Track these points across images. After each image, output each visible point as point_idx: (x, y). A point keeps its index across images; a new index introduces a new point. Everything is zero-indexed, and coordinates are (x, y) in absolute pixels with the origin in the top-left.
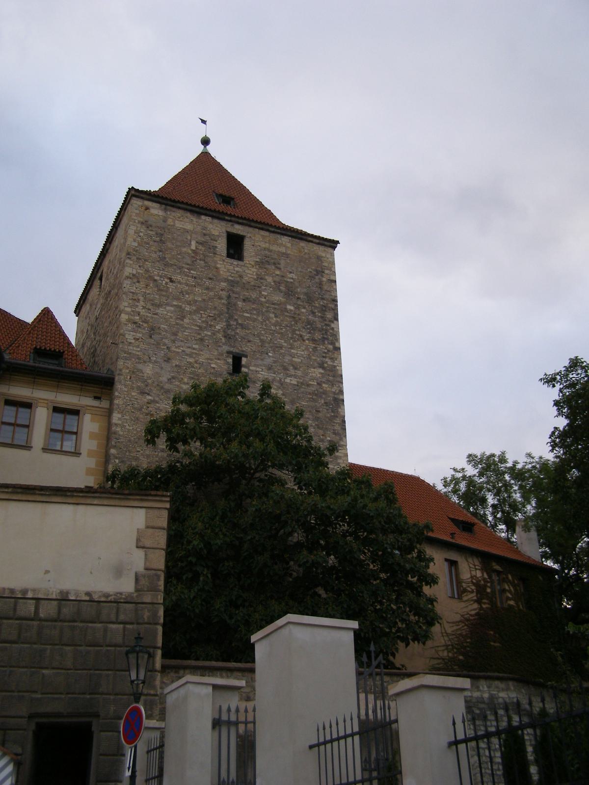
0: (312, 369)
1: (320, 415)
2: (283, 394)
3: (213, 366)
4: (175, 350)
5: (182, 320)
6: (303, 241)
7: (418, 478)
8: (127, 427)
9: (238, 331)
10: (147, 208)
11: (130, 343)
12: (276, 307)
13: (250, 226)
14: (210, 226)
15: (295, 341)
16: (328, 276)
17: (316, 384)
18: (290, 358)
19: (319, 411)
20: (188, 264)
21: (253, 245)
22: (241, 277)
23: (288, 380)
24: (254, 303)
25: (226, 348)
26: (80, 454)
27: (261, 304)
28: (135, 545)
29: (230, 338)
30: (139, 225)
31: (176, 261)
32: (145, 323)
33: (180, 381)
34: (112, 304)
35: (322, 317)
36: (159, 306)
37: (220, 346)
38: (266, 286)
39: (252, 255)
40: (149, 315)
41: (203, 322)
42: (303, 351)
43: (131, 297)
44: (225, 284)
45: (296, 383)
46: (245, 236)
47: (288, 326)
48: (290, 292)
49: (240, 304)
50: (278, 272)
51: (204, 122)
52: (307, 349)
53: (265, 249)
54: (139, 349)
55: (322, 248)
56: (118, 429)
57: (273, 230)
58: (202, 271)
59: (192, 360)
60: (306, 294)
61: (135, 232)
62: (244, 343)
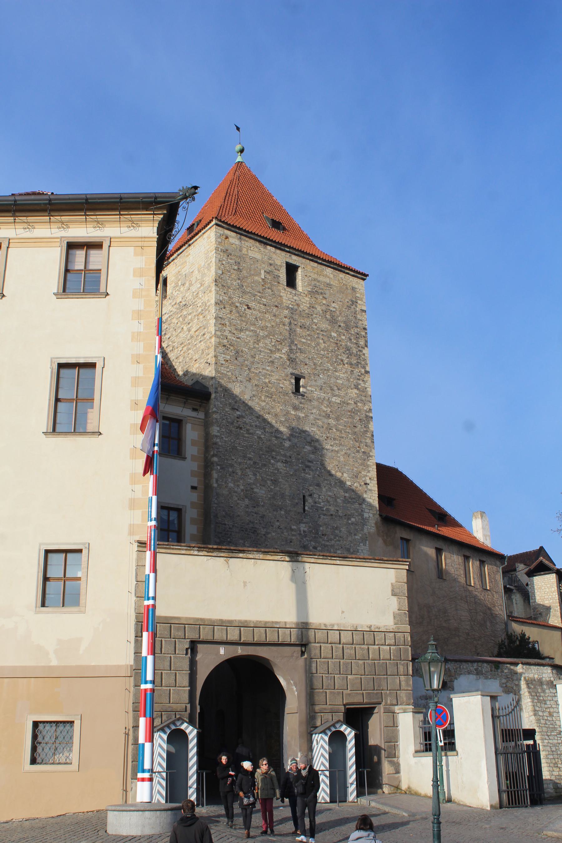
0: (351, 390)
1: (356, 430)
2: (331, 412)
3: (282, 386)
4: (254, 371)
5: (258, 344)
6: (342, 273)
7: (397, 470)
8: (224, 439)
9: (298, 355)
10: (227, 238)
11: (222, 364)
12: (324, 333)
13: (304, 258)
14: (274, 256)
15: (338, 365)
16: (360, 306)
17: (353, 403)
18: (335, 380)
19: (355, 427)
20: (260, 292)
21: (306, 276)
22: (298, 305)
23: (334, 399)
24: (308, 330)
25: (290, 370)
26: (186, 458)
27: (314, 331)
28: (390, 593)
29: (292, 361)
30: (222, 254)
31: (251, 289)
32: (232, 346)
33: (259, 399)
34: (192, 320)
35: (357, 344)
36: (241, 330)
37: (285, 368)
38: (316, 314)
39: (305, 285)
40: (234, 339)
41: (273, 346)
42: (344, 373)
43: (220, 322)
44: (287, 312)
45: (339, 402)
46: (300, 266)
47: (332, 351)
48: (333, 321)
49: (298, 330)
50: (324, 302)
51: (238, 129)
52: (346, 372)
53: (315, 280)
54: (228, 370)
55: (356, 280)
56: (218, 440)
57: (320, 261)
58: (270, 300)
59: (267, 381)
60: (345, 322)
61: (219, 260)
62: (302, 366)
